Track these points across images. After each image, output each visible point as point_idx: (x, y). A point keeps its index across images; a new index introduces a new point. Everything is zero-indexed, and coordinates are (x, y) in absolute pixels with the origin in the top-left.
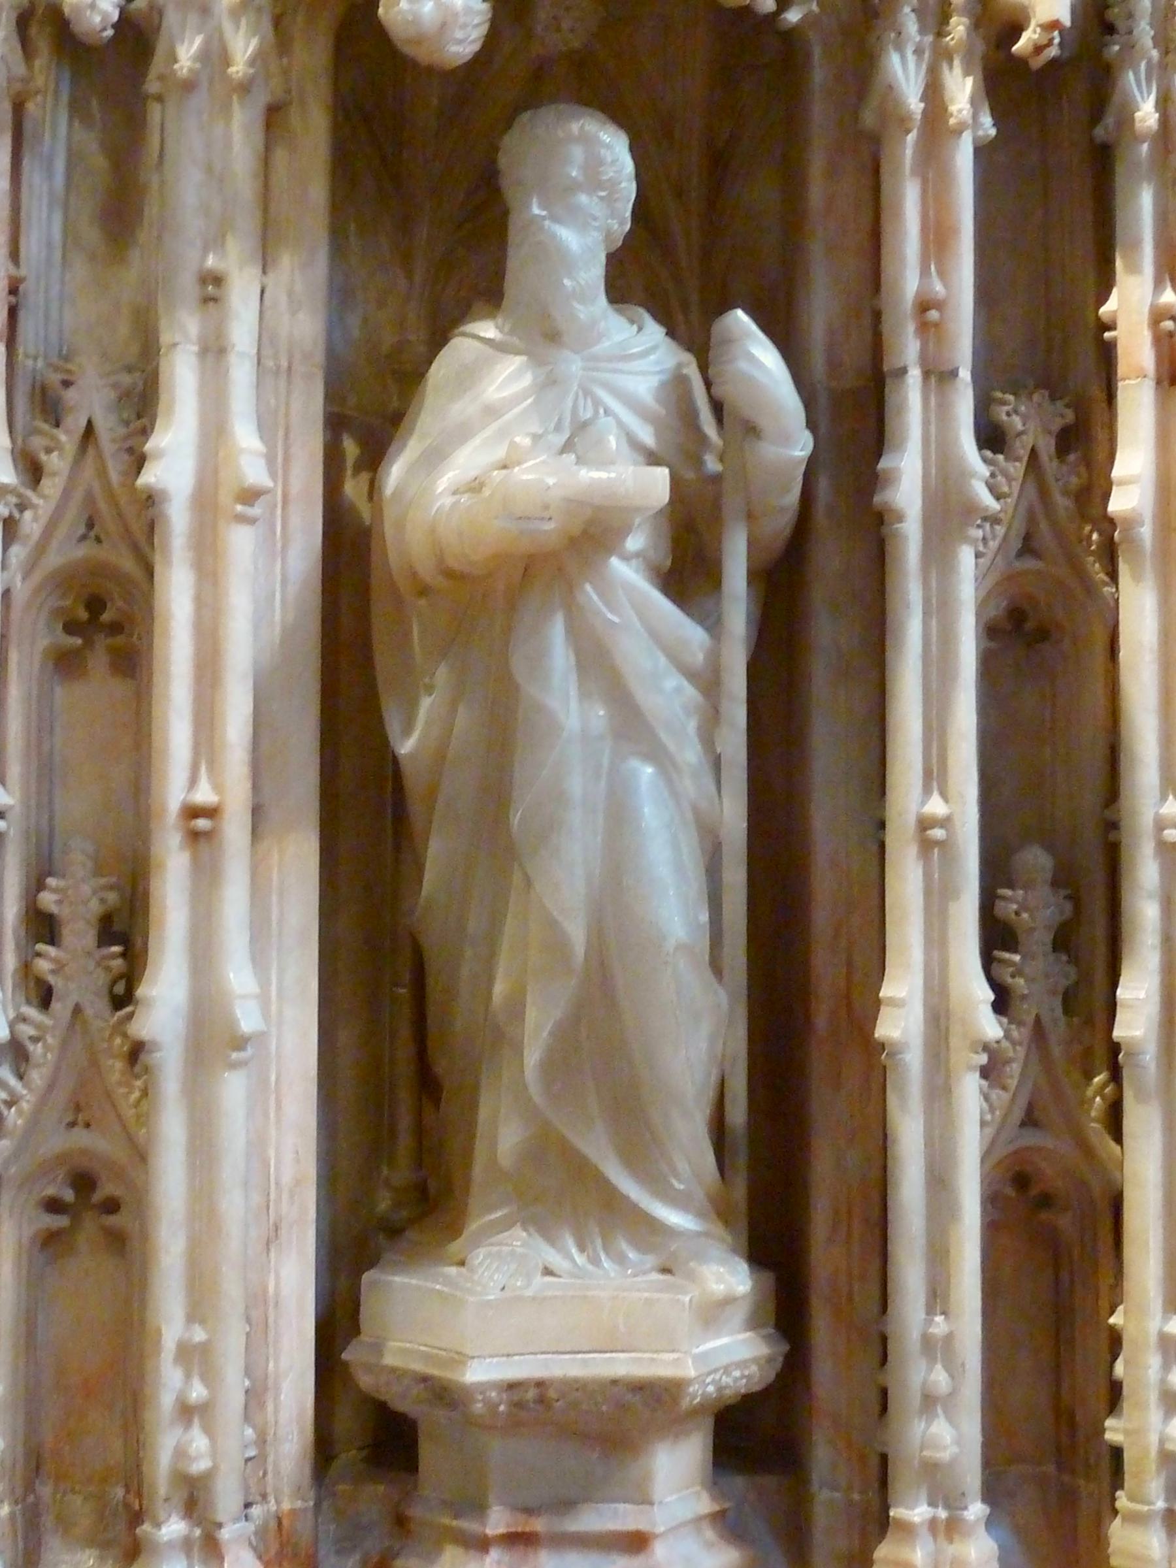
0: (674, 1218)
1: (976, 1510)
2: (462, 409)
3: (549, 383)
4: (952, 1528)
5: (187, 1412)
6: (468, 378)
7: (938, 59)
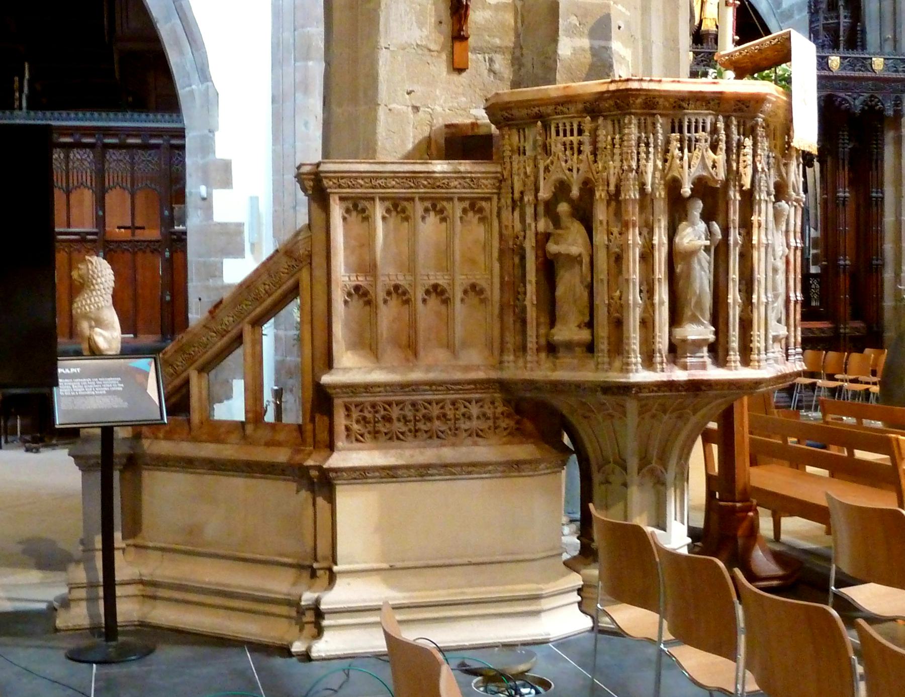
0: (705, 322)
1: (738, 353)
2: (685, 233)
3: (694, 230)
4: (735, 355)
5: (659, 342)
6: (684, 230)
7: (735, 191)
